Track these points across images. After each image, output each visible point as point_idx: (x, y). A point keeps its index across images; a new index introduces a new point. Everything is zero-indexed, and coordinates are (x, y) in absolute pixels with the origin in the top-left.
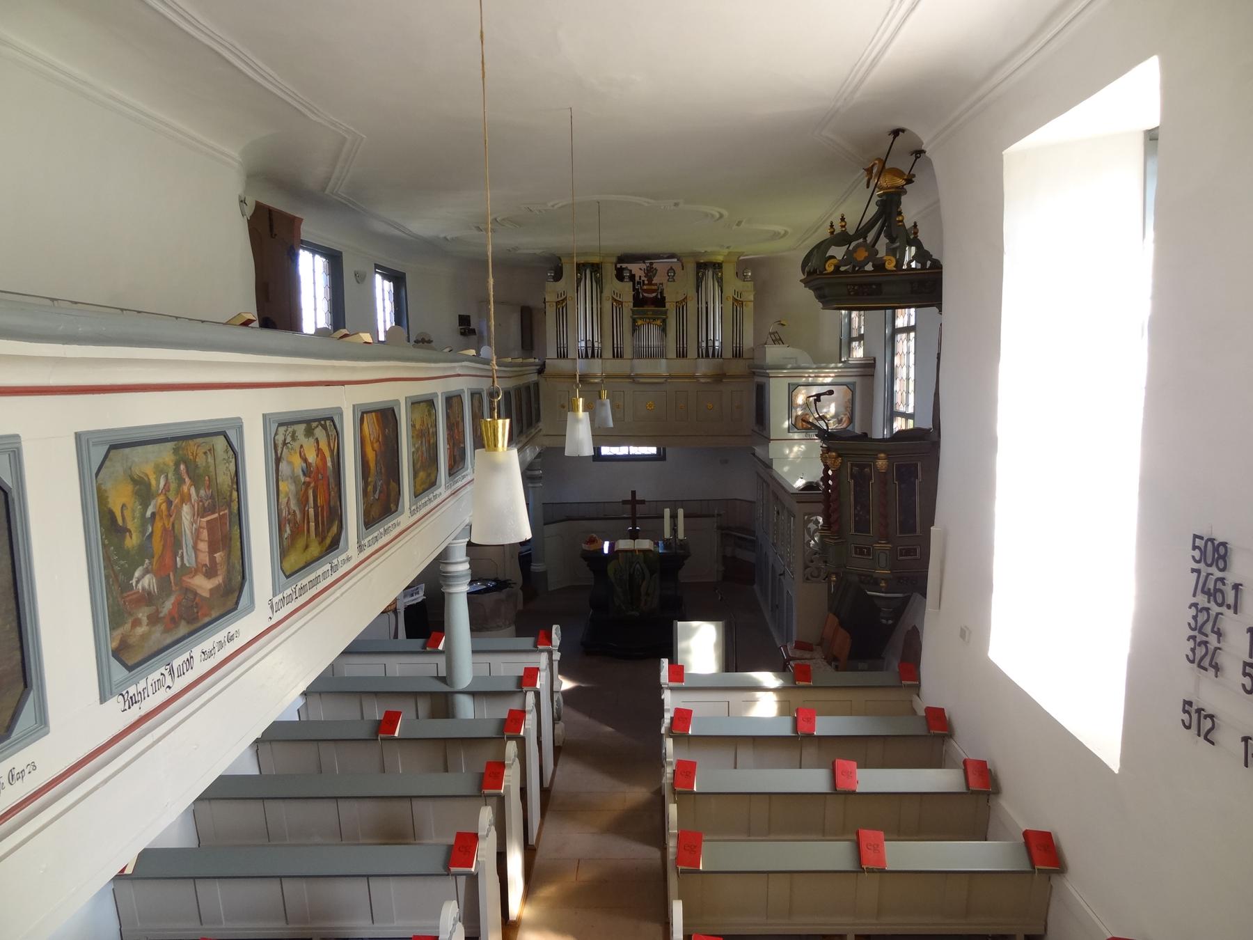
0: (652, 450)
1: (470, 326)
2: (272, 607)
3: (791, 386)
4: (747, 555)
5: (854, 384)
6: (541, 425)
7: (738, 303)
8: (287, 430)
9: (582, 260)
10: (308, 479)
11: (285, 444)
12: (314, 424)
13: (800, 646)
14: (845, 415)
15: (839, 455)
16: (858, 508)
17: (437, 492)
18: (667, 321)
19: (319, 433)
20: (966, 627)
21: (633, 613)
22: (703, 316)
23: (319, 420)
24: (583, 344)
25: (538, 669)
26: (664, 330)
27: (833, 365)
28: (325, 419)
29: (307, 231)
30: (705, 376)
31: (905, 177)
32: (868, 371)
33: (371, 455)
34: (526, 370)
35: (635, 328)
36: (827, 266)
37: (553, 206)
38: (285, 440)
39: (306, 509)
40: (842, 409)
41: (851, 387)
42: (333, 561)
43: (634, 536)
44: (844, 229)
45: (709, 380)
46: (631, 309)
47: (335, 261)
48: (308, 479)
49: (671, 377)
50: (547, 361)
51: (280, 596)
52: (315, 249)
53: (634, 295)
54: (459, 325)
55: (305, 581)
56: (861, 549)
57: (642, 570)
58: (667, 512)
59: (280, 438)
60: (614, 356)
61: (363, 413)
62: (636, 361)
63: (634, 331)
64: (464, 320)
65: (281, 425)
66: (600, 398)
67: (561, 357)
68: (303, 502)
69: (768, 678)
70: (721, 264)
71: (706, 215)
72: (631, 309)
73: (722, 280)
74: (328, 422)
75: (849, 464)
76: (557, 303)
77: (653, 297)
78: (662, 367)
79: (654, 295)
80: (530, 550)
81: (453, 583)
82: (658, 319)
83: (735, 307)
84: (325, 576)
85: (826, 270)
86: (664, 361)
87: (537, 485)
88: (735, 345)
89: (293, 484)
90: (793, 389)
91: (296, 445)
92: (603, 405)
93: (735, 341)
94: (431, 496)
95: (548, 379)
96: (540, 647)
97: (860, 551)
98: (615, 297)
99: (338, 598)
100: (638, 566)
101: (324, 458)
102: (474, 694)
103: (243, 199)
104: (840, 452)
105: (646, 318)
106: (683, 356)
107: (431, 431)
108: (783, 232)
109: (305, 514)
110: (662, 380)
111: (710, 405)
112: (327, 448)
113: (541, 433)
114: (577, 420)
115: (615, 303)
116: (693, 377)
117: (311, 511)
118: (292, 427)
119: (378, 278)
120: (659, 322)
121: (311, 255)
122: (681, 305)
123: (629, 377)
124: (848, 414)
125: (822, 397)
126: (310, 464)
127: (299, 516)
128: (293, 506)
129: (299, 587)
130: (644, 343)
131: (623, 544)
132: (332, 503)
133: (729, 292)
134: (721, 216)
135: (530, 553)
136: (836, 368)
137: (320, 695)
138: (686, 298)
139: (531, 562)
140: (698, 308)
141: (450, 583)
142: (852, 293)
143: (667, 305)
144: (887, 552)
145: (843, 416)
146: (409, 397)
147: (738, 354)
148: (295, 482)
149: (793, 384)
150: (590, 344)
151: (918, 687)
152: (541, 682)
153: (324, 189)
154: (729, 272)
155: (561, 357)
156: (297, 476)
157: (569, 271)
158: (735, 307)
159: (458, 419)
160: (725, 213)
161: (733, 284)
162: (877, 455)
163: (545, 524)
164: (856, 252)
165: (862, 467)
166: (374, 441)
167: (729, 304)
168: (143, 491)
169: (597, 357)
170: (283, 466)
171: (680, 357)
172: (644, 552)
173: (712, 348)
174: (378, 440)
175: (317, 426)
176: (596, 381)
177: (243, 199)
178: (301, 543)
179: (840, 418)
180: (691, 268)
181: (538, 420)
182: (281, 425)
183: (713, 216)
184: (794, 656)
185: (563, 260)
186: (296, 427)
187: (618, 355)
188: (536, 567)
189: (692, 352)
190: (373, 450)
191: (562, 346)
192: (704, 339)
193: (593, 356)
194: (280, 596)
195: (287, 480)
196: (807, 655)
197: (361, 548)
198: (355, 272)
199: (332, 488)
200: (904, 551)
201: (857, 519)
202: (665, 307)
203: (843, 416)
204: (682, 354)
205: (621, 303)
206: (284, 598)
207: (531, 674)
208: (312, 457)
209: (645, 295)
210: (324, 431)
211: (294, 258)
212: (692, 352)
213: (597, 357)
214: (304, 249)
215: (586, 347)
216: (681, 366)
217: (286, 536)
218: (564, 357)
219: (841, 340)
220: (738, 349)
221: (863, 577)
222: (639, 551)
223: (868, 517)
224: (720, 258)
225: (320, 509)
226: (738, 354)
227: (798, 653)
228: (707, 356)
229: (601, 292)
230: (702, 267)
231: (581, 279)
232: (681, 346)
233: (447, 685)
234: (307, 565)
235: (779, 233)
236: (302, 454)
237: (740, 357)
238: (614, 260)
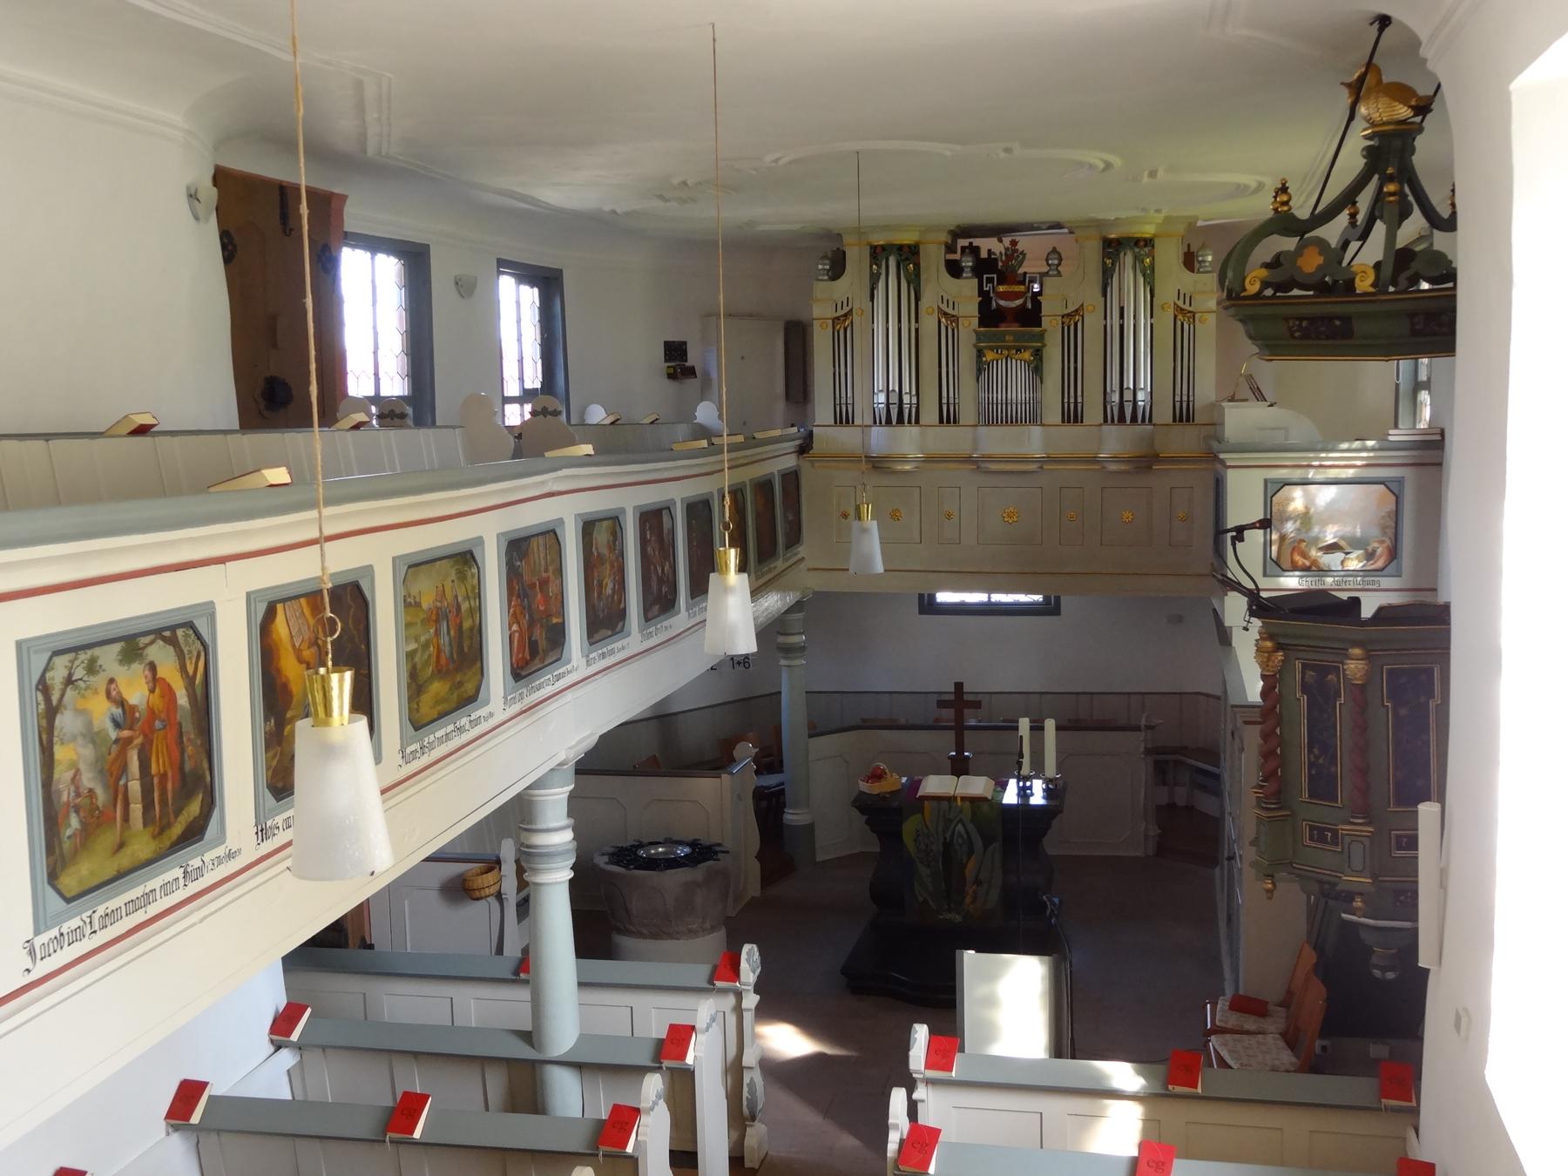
0: (1038, 598)
1: (686, 361)
2: (32, 953)
3: (1269, 484)
4: (1206, 803)
5: (1400, 481)
6: (802, 550)
7: (1185, 315)
8: (76, 659)
9: (880, 239)
10: (126, 733)
11: (69, 681)
12: (143, 641)
13: (1242, 1005)
14: (1382, 542)
15: (1279, 647)
16: (1316, 751)
17: (482, 712)
19: (160, 654)
20: (1466, 1010)
21: (948, 916)
22: (1115, 343)
23: (158, 633)
24: (882, 398)
25: (693, 1028)
26: (1037, 369)
27: (1345, 446)
28: (173, 628)
29: (354, 217)
30: (1116, 459)
31: (1413, 103)
32: (1428, 456)
34: (776, 450)
35: (981, 368)
36: (1247, 281)
37: (776, 161)
38: (70, 675)
39: (122, 782)
40: (1375, 532)
41: (1394, 488)
42: (190, 863)
43: (960, 767)
44: (1286, 208)
45: (1123, 467)
46: (974, 330)
47: (416, 260)
48: (126, 733)
49: (1050, 459)
50: (815, 430)
51: (54, 932)
52: (374, 244)
53: (980, 303)
54: (666, 361)
55: (116, 902)
56: (1322, 831)
57: (967, 832)
58: (1024, 724)
59: (57, 676)
60: (941, 421)
62: (983, 430)
63: (981, 373)
64: (675, 351)
65: (58, 653)
66: (860, 519)
67: (841, 422)
68: (113, 772)
69: (1122, 1074)
70: (1151, 240)
71: (1081, 164)
72: (974, 330)
73: (1153, 270)
74: (180, 632)
75: (1298, 665)
76: (835, 320)
77: (1017, 307)
78: (1033, 441)
79: (1019, 302)
80: (783, 784)
81: (540, 866)
82: (1026, 348)
83: (1179, 323)
84: (167, 889)
85: (1245, 290)
86: (1036, 431)
87: (797, 662)
88: (1178, 398)
89: (90, 746)
90: (1273, 489)
91: (99, 681)
92: (865, 531)
93: (1178, 391)
94: (464, 721)
95: (816, 464)
96: (719, 984)
97: (1319, 834)
98: (944, 307)
99: (194, 925)
100: (960, 825)
101: (169, 694)
102: (579, 1067)
103: (193, 193)
104: (1281, 641)
105: (1002, 348)
106: (1076, 421)
107: (465, 606)
108: (1254, 185)
109: (118, 794)
110: (1033, 467)
111: (1127, 515)
112: (178, 675)
113: (802, 566)
114: (726, 589)
115: (943, 320)
116: (1094, 460)
117: (135, 787)
118: (89, 652)
119: (506, 283)
120: (1027, 355)
121: (369, 254)
122: (1072, 319)
123: (968, 460)
124: (1388, 542)
125: (1246, 533)
126: (133, 708)
127: (101, 796)
128: (88, 780)
129: (101, 910)
130: (999, 396)
131: (935, 785)
132: (188, 767)
133: (1167, 294)
134: (1108, 165)
135: (783, 789)
136: (1365, 449)
137: (324, 1050)
138: (1082, 305)
139: (785, 806)
140: (1105, 326)
141: (540, 866)
142: (1297, 334)
143: (1045, 322)
144: (1367, 842)
145: (1376, 545)
147: (1183, 415)
148: (94, 742)
149: (1274, 481)
150: (894, 399)
151: (1415, 1112)
152: (703, 1055)
153: (365, 151)
154: (1168, 257)
155: (841, 422)
156: (98, 733)
157: (856, 259)
158: (1179, 323)
159: (544, 575)
160: (1117, 161)
161: (1173, 278)
162: (1347, 650)
163: (811, 736)
164: (1301, 256)
165: (1323, 671)
166: (305, 646)
167: (1166, 319)
169: (910, 422)
170: (66, 722)
171: (1069, 421)
172: (975, 801)
173: (1131, 404)
175: (152, 643)
176: (907, 467)
177: (193, 193)
178: (108, 838)
179: (1370, 549)
180: (1093, 250)
181: (795, 537)
182: (58, 653)
183: (1091, 166)
184: (1223, 1025)
185: (847, 239)
186: (97, 651)
187: (948, 418)
188: (792, 816)
189: (1093, 413)
191: (843, 401)
192: (1116, 387)
193: (900, 421)
194: (54, 932)
195: (74, 739)
196: (1251, 1023)
197: (263, 833)
198: (455, 277)
199: (189, 740)
200: (1405, 840)
201: (1313, 772)
202: (1040, 325)
203: (1376, 545)
204: (1072, 416)
205: (954, 319)
206: (62, 934)
207: (680, 1036)
208: (137, 693)
209: (1002, 303)
210: (171, 649)
211: (327, 265)
212: (1093, 413)
213: (910, 422)
214: (354, 247)
215: (888, 404)
216: (1071, 439)
217: (68, 832)
218: (847, 422)
219: (1397, 386)
220: (1185, 405)
221: (1327, 886)
222: (963, 799)
223: (1333, 769)
224: (1148, 230)
225: (156, 780)
226: (1183, 415)
227: (1233, 1020)
228: (1122, 419)
229: (917, 299)
230: (1113, 248)
231: (879, 274)
232: (1072, 400)
233: (533, 1047)
234: (121, 875)
235: (1246, 187)
236: (114, 693)
237: (1188, 420)
238: (944, 237)
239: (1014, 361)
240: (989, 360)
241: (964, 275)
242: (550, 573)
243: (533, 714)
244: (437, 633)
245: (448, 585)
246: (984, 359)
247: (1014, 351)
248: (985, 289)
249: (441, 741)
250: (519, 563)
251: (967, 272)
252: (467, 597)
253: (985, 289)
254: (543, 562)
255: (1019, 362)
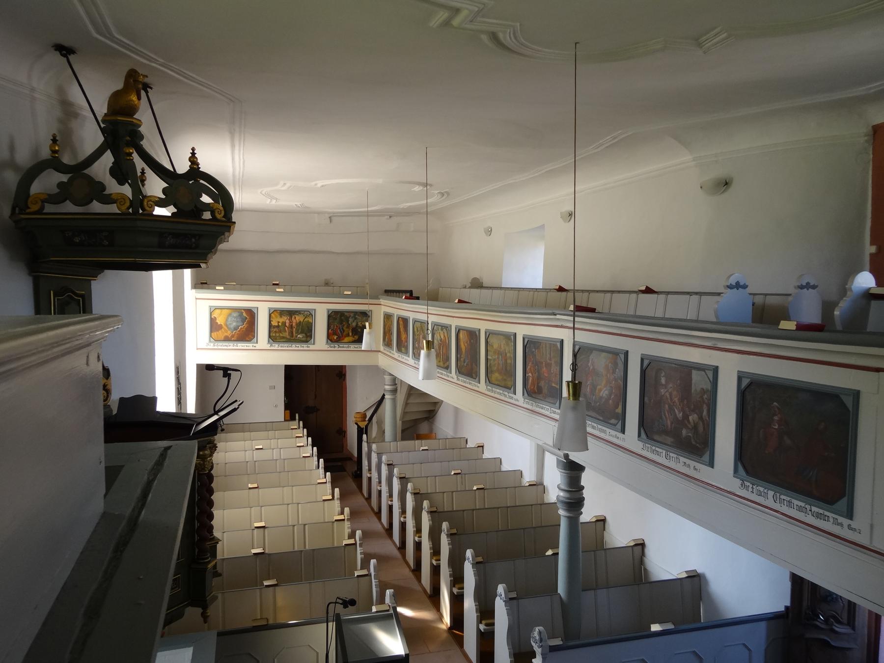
12: (443, 328)
33: (463, 347)
61: (459, 331)
101: (446, 339)
146: (434, 322)
168: (417, 330)
170: (435, 336)
174: (467, 343)
190: (464, 345)
208: (442, 337)
242: (553, 362)
243: (532, 414)
244: (498, 358)
245: (502, 346)
249: (498, 393)
250: (534, 350)
252: (509, 352)
254: (548, 355)
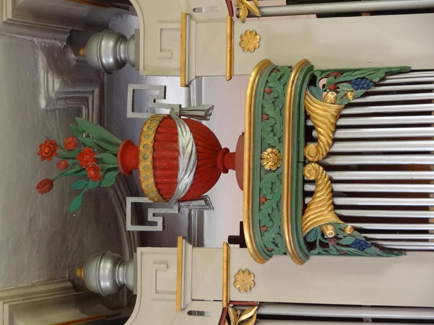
18: (319, 65)
239: (339, 147)
240: (332, 218)
241: (130, 283)
246: (330, 232)
247: (312, 146)
248: (159, 228)
251: (126, 275)
253: (159, 228)
255: (341, 133)
